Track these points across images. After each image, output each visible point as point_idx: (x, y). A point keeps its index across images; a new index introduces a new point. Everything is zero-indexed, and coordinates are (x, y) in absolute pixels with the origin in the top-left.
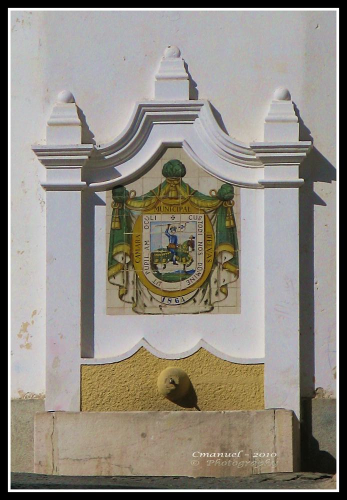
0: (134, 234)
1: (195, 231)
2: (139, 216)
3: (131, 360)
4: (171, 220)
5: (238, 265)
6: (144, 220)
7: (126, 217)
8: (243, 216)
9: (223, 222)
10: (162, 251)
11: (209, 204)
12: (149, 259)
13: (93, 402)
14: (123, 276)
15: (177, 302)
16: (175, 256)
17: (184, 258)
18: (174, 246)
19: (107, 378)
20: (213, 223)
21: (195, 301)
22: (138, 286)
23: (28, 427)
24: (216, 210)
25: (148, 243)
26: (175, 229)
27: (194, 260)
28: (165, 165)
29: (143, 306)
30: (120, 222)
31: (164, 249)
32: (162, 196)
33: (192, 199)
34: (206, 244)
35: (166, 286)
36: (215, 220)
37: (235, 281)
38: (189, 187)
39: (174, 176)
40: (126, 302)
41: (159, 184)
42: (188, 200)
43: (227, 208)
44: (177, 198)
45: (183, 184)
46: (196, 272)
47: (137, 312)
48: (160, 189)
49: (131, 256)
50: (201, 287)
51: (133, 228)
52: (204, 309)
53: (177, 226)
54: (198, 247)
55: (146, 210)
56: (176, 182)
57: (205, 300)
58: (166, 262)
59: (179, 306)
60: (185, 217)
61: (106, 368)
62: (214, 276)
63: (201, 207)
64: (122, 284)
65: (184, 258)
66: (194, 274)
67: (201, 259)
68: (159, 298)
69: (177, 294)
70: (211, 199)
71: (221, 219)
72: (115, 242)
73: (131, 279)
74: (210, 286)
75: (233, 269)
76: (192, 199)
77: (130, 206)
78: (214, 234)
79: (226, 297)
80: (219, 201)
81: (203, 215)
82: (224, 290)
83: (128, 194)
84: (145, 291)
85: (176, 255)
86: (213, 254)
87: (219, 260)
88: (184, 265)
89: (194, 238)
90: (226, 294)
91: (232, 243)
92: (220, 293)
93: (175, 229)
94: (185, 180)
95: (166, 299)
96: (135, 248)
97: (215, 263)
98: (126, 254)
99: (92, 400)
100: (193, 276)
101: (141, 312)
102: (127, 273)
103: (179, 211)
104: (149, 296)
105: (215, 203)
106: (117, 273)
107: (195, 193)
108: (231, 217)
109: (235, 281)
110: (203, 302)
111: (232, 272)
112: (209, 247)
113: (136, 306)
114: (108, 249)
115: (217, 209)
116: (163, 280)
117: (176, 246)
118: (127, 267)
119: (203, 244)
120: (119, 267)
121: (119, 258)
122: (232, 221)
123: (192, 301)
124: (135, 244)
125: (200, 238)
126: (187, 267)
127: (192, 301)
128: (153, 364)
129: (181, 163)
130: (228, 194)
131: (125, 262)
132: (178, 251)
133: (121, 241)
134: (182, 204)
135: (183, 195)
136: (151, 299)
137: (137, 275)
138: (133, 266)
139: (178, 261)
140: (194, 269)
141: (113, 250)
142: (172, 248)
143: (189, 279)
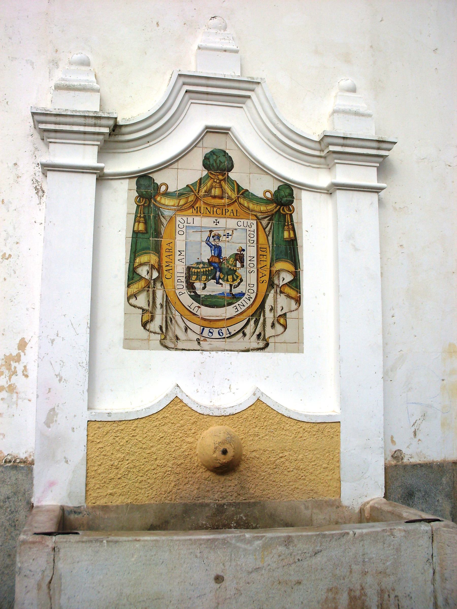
0: (164, 242)
1: (245, 241)
3: (160, 417)
4: (214, 225)
5: (300, 289)
6: (178, 223)
7: (155, 217)
8: (305, 226)
9: (280, 233)
10: (201, 266)
11: (263, 208)
12: (184, 275)
13: (104, 475)
14: (148, 296)
15: (221, 334)
16: (218, 273)
17: (231, 276)
19: (124, 441)
20: (268, 233)
21: (244, 335)
22: (169, 312)
23: (7, 506)
25: (183, 253)
26: (219, 237)
27: (244, 279)
28: (206, 154)
29: (174, 339)
30: (146, 223)
31: (204, 263)
32: (202, 193)
33: (241, 201)
34: (260, 259)
36: (271, 229)
37: (296, 310)
38: (237, 184)
40: (151, 332)
41: (199, 178)
42: (235, 201)
43: (285, 215)
44: (222, 198)
46: (246, 296)
47: (167, 347)
48: (200, 184)
49: (159, 270)
50: (252, 316)
51: (162, 232)
52: (256, 346)
53: (221, 233)
54: (249, 262)
55: (180, 209)
56: (221, 177)
57: (257, 333)
58: (207, 280)
59: (224, 340)
60: (232, 223)
61: (124, 426)
62: (269, 302)
63: (252, 211)
64: (146, 307)
65: (231, 276)
66: (244, 298)
68: (197, 329)
69: (220, 324)
70: (265, 201)
71: (278, 228)
72: (138, 250)
73: (159, 300)
74: (264, 316)
75: (293, 293)
76: (241, 201)
77: (160, 203)
78: (269, 247)
79: (285, 331)
80: (275, 205)
81: (255, 222)
82: (282, 321)
83: (157, 187)
84: (178, 318)
85: (221, 271)
86: (267, 273)
87: (276, 282)
88: (231, 286)
89: (243, 250)
90: (285, 327)
92: (277, 325)
93: (219, 237)
94: (232, 175)
95: (206, 330)
96: (165, 259)
97: (271, 284)
98: (153, 267)
99: (103, 473)
100: (241, 300)
101: (172, 346)
102: (154, 293)
103: (224, 215)
104: (182, 325)
105: (271, 207)
106: (140, 292)
108: (291, 227)
109: (296, 310)
110: (255, 336)
111: (292, 298)
112: (263, 264)
113: (165, 338)
114: (129, 258)
115: (273, 215)
116: (202, 305)
117: (219, 259)
118: (154, 284)
119: (255, 259)
120: (142, 284)
121: (143, 271)
122: (292, 232)
123: (241, 334)
124: (164, 254)
125: (251, 252)
126: (234, 288)
127: (241, 334)
128: (192, 421)
130: (286, 197)
131: (151, 277)
132: (223, 266)
133: (146, 250)
134: (229, 205)
135: (230, 194)
136: (186, 330)
137: (167, 296)
138: (162, 284)
139: (223, 279)
140: (244, 292)
141: (135, 260)
142: (215, 263)
143: (236, 304)
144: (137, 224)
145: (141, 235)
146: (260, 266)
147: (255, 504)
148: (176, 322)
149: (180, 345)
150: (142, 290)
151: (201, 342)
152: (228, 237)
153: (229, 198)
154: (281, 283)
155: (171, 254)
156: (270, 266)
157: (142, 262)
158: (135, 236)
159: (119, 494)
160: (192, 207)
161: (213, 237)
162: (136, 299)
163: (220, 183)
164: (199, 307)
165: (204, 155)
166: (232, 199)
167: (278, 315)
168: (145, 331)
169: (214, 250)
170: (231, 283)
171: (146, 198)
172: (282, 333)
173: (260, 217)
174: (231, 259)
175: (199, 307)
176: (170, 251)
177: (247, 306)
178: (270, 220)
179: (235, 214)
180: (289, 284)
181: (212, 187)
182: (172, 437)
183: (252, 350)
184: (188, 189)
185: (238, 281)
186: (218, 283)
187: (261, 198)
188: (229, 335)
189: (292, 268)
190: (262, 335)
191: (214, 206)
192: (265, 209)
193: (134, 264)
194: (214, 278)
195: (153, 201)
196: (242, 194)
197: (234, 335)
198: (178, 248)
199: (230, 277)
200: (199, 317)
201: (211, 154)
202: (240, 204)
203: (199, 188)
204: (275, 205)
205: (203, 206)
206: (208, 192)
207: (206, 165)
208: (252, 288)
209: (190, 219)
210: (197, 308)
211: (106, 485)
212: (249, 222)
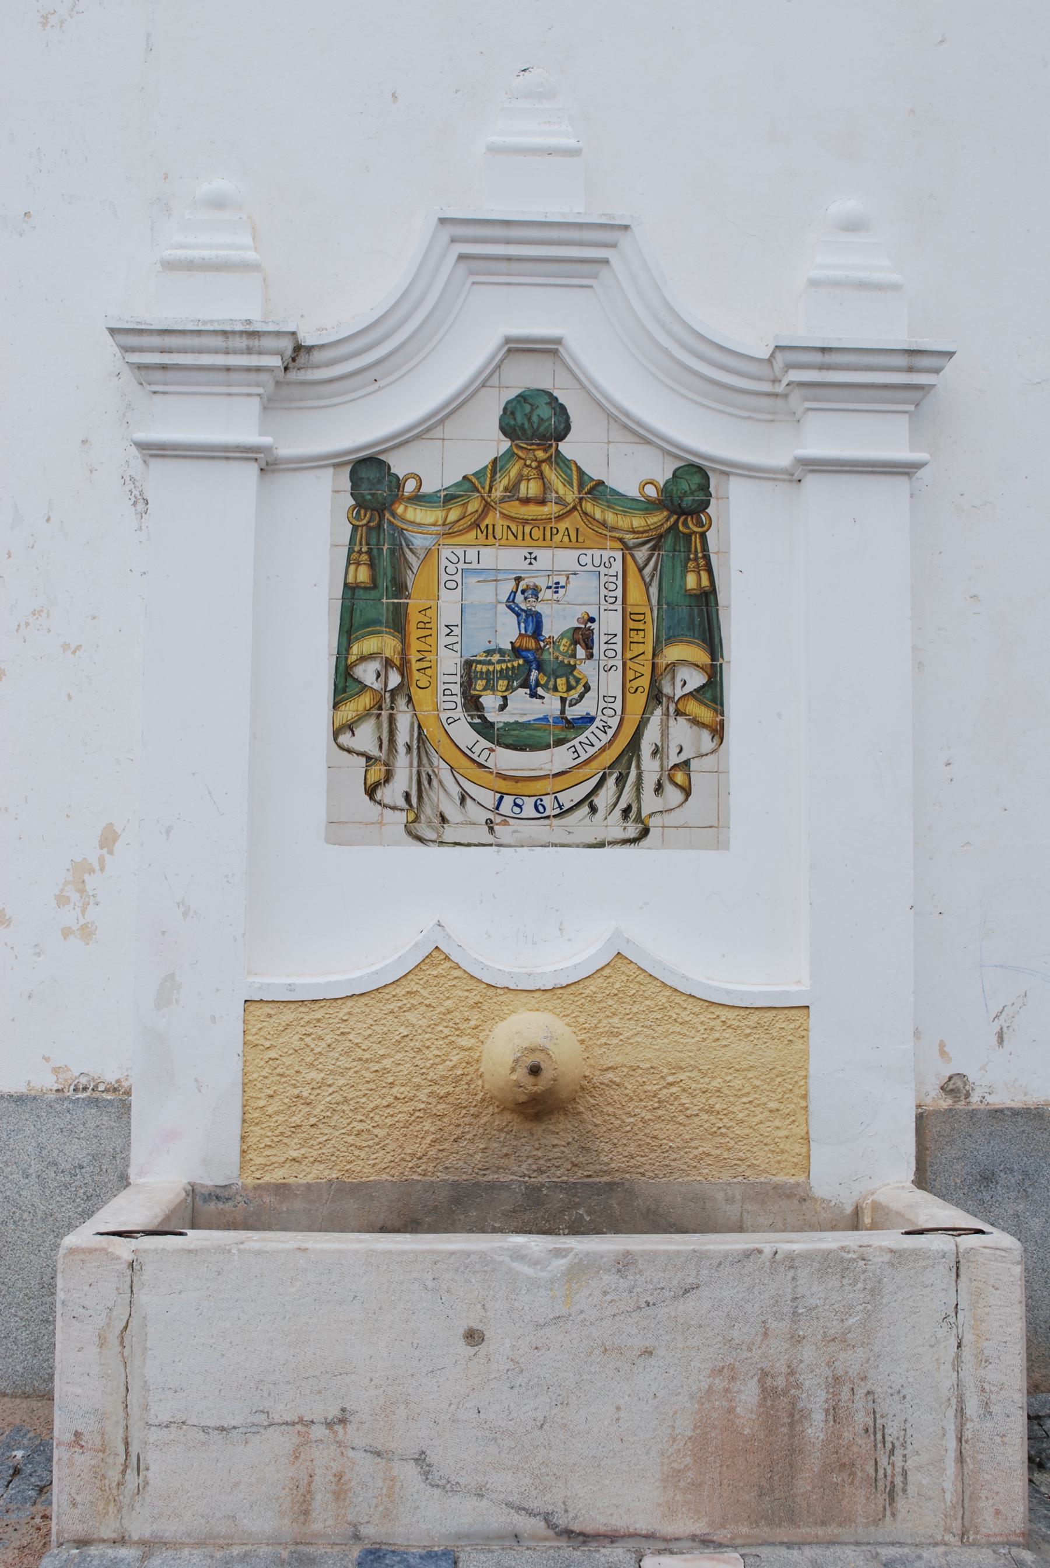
0: (414, 604)
2: (429, 551)
3: (400, 991)
4: (525, 565)
5: (722, 705)
6: (444, 563)
7: (392, 551)
8: (736, 559)
10: (496, 657)
11: (638, 522)
12: (457, 679)
13: (280, 1118)
14: (379, 727)
15: (541, 809)
16: (534, 674)
17: (564, 679)
18: (531, 644)
19: (323, 1044)
20: (648, 580)
21: (593, 809)
22: (425, 761)
23: (77, 1183)
24: (657, 542)
25: (457, 631)
26: (536, 591)
27: (593, 685)
28: (508, 403)
29: (436, 821)
30: (372, 566)
31: (501, 652)
32: (498, 493)
33: (588, 506)
34: (629, 640)
35: (507, 760)
36: (655, 569)
37: (713, 752)
38: (579, 468)
39: (534, 435)
40: (385, 806)
41: (493, 457)
42: (574, 508)
43: (690, 535)
44: (542, 502)
45: (559, 461)
46: (597, 723)
47: (420, 839)
48: (494, 473)
52: (619, 834)
53: (542, 582)
54: (604, 647)
55: (450, 531)
56: (540, 454)
57: (622, 804)
58: (510, 688)
59: (547, 822)
60: (566, 559)
61: (323, 1011)
62: (651, 736)
63: (614, 529)
64: (374, 752)
65: (564, 679)
66: (593, 728)
67: (613, 683)
70: (644, 506)
71: (673, 567)
72: (356, 625)
73: (403, 737)
74: (638, 767)
75: (705, 714)
76: (588, 506)
77: (403, 519)
78: (652, 611)
79: (686, 800)
80: (665, 513)
81: (618, 555)
82: (680, 777)
83: (398, 484)
84: (445, 774)
85: (539, 668)
86: (647, 671)
87: (667, 689)
88: (563, 700)
89: (592, 620)
90: (687, 792)
91: (704, 641)
92: (669, 788)
93: (536, 591)
94: (566, 448)
95: (508, 801)
96: (415, 645)
97: (656, 696)
98: (388, 663)
99: (277, 1113)
100: (587, 733)
101: (433, 836)
102: (392, 719)
104: (455, 791)
105: (656, 519)
106: (360, 719)
107: (597, 490)
108: (702, 562)
109: (713, 752)
110: (617, 813)
111: (704, 725)
112: (637, 649)
113: (416, 820)
114: (336, 645)
115: (660, 537)
116: (499, 744)
117: (537, 641)
118: (393, 701)
119: (619, 639)
120: (365, 700)
121: (367, 673)
122: (704, 576)
123: (585, 809)
124: (414, 633)
125: (610, 623)
126: (571, 705)
127: (585, 809)
128: (471, 1002)
129: (556, 399)
130: (692, 493)
131: (386, 685)
132: (545, 656)
133: (371, 626)
134: (560, 518)
135: (561, 492)
136: (463, 800)
137: (420, 727)
139: (545, 687)
140: (593, 713)
141: (348, 648)
142: (528, 650)
143: (575, 742)
144: (352, 568)
145: (361, 592)
146: (629, 655)
147: (611, 1186)
148: (441, 782)
149: (450, 834)
150: (367, 714)
151: (496, 827)
152: (556, 592)
153: (560, 501)
154: (679, 693)
155: (428, 632)
156: (654, 655)
157: (365, 653)
158: (349, 594)
159: (312, 1159)
160: (476, 525)
161: (523, 592)
162: (353, 734)
163: (539, 467)
164: (492, 750)
165: (502, 406)
166: (566, 505)
167: (671, 764)
168: (372, 803)
169: (526, 622)
170: (565, 695)
171: (372, 510)
172: (681, 805)
173: (631, 543)
174: (564, 641)
175: (492, 750)
176: (428, 626)
177: (598, 745)
178: (654, 549)
179: (574, 539)
180: (697, 694)
181: (520, 478)
182: (427, 1036)
183: (610, 843)
184: (467, 485)
185: (580, 689)
186: (534, 695)
187: (633, 500)
188: (558, 811)
189: (704, 658)
190: (634, 809)
191: (525, 522)
192: (643, 523)
193: (347, 658)
194: (525, 684)
195: (387, 515)
196: (589, 492)
197: (571, 809)
198: (445, 619)
199: (561, 682)
200: (491, 773)
201: (519, 402)
202: (586, 514)
203: (491, 482)
204: (665, 513)
205: (500, 523)
206: (512, 490)
207: (507, 430)
208: (610, 705)
209: (472, 554)
210: (487, 752)
211: (285, 1140)
212: (606, 554)
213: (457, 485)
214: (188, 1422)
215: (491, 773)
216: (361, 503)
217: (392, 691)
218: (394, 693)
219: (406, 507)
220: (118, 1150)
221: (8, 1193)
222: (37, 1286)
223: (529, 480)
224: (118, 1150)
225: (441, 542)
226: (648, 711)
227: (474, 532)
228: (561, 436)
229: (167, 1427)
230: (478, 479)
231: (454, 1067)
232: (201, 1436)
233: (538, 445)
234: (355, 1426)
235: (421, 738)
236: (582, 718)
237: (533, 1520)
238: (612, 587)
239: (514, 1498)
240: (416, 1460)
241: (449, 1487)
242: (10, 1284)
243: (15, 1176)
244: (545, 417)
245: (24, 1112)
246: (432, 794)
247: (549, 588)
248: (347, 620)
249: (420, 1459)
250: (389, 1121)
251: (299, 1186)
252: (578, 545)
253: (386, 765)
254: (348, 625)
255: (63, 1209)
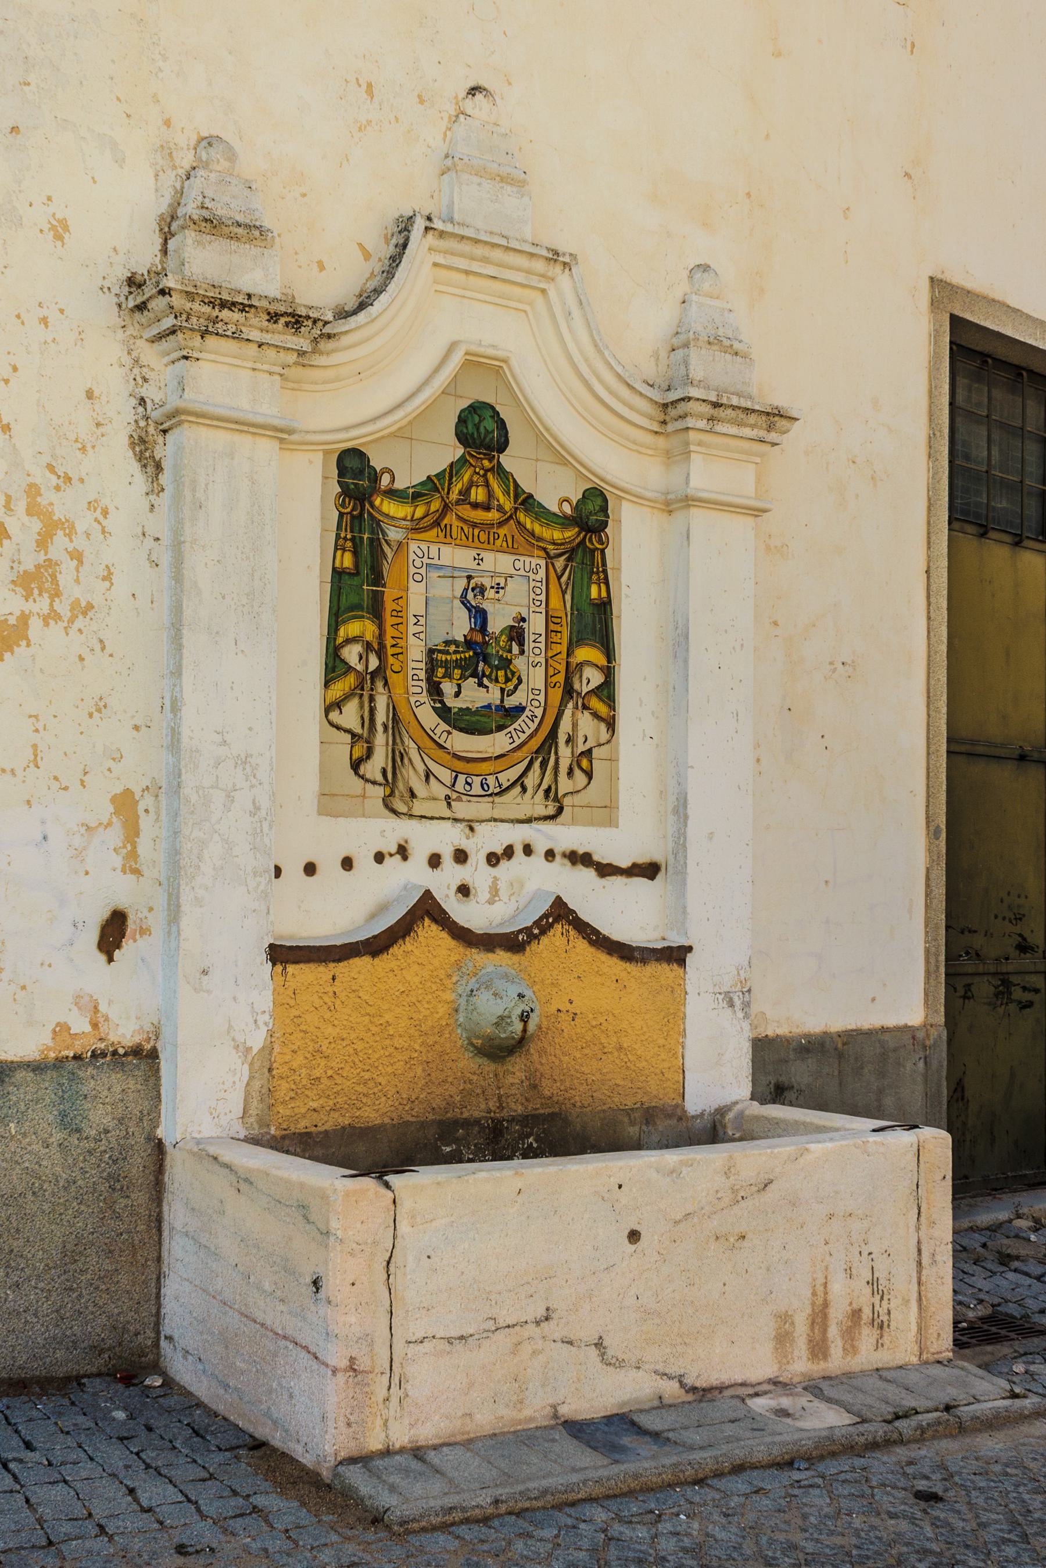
0: (389, 594)
1: (525, 601)
2: (400, 544)
4: (473, 565)
5: (614, 702)
6: (412, 556)
7: (371, 540)
9: (585, 589)
10: (453, 648)
11: (557, 535)
12: (423, 665)
14: (362, 706)
16: (481, 664)
18: (479, 638)
21: (524, 789)
22: (398, 740)
23: (103, 1148)
24: (571, 554)
25: (422, 621)
26: (481, 590)
27: (524, 678)
28: (462, 411)
29: (407, 795)
30: (356, 553)
31: (455, 642)
33: (521, 516)
35: (462, 742)
36: (569, 578)
37: (608, 742)
38: (515, 481)
39: (482, 445)
40: (367, 781)
42: (511, 517)
44: (487, 508)
45: (500, 472)
46: (527, 713)
47: (394, 812)
49: (381, 653)
50: (537, 752)
51: (385, 574)
52: (541, 811)
53: (487, 582)
54: (532, 645)
55: (417, 527)
56: (486, 463)
57: (545, 786)
59: (490, 799)
60: (504, 562)
62: (565, 727)
63: (540, 539)
64: (358, 730)
66: (523, 717)
67: (537, 678)
68: (446, 776)
69: (485, 767)
70: (561, 521)
73: (381, 717)
74: (556, 753)
75: (602, 709)
76: (521, 516)
77: (380, 512)
79: (589, 783)
80: (577, 529)
81: (543, 563)
82: (585, 763)
83: (375, 477)
85: (485, 661)
86: (562, 668)
88: (502, 690)
89: (523, 620)
90: (589, 775)
91: (602, 645)
92: (577, 772)
95: (462, 778)
96: (390, 632)
97: (569, 692)
98: (368, 646)
100: (520, 721)
102: (372, 699)
103: (490, 544)
104: (421, 768)
105: (570, 533)
106: (347, 698)
107: (527, 502)
108: (602, 576)
109: (608, 742)
110: (541, 793)
112: (556, 648)
113: (392, 794)
116: (455, 728)
118: (372, 683)
119: (542, 639)
120: (351, 680)
121: (352, 654)
122: (603, 587)
123: (518, 789)
124: (389, 621)
125: (536, 624)
126: (508, 696)
127: (518, 789)
129: (498, 414)
130: (596, 514)
131: (367, 668)
133: (355, 610)
134: (501, 524)
135: (502, 501)
138: (386, 684)
139: (489, 677)
140: (524, 704)
141: (337, 630)
142: (476, 643)
143: (511, 729)
144: (339, 553)
145: (347, 577)
146: (550, 654)
147: (553, 1115)
148: (410, 760)
149: (418, 808)
150: (352, 694)
151: (453, 803)
152: (498, 592)
153: (500, 509)
154: (585, 690)
155: (399, 620)
156: (568, 655)
157: (350, 636)
158: (336, 580)
159: (328, 1108)
160: (437, 523)
161: (473, 589)
162: (341, 713)
163: (485, 475)
164: (449, 733)
165: (458, 414)
166: (505, 513)
167: (579, 752)
168: (356, 778)
169: (475, 617)
170: (503, 686)
171: (356, 499)
172: (585, 788)
173: (552, 553)
174: (503, 637)
175: (449, 733)
176: (400, 614)
177: (528, 732)
178: (569, 559)
179: (510, 545)
180: (596, 692)
181: (471, 484)
182: (420, 991)
183: (536, 819)
184: (430, 485)
185: (515, 681)
186: (481, 684)
187: (554, 514)
188: (498, 790)
189: (602, 661)
190: (553, 789)
191: (474, 525)
192: (561, 537)
193: (335, 639)
194: (474, 675)
195: (367, 505)
196: (522, 504)
197: (508, 788)
198: (412, 611)
199: (501, 673)
200: (449, 753)
201: (470, 412)
202: (519, 523)
203: (450, 484)
204: (577, 529)
205: (456, 523)
206: (465, 492)
207: (463, 438)
208: (537, 697)
209: (434, 549)
210: (445, 734)
211: (307, 1092)
212: (535, 561)
213: (422, 484)
214: (438, 1336)
215: (449, 753)
216: (346, 492)
217: (371, 673)
218: (374, 675)
219: (382, 500)
220: (145, 1112)
221: (27, 1164)
222: (59, 1256)
223: (478, 486)
224: (145, 1112)
225: (410, 536)
226: (563, 704)
227: (435, 530)
228: (502, 449)
229: (421, 1342)
230: (439, 480)
231: (441, 1018)
232: (447, 1347)
233: (484, 454)
234: (555, 1322)
235: (396, 719)
236: (517, 707)
237: (671, 1383)
238: (538, 591)
239: (660, 1367)
240: (596, 1345)
241: (618, 1364)
242: (30, 1256)
243: (34, 1146)
244: (490, 429)
245: (44, 1080)
246: (403, 770)
247: (492, 587)
248: (335, 603)
249: (599, 1345)
250: (390, 1070)
251: (320, 1133)
252: (513, 551)
253: (368, 742)
254: (335, 608)
255: (88, 1175)
